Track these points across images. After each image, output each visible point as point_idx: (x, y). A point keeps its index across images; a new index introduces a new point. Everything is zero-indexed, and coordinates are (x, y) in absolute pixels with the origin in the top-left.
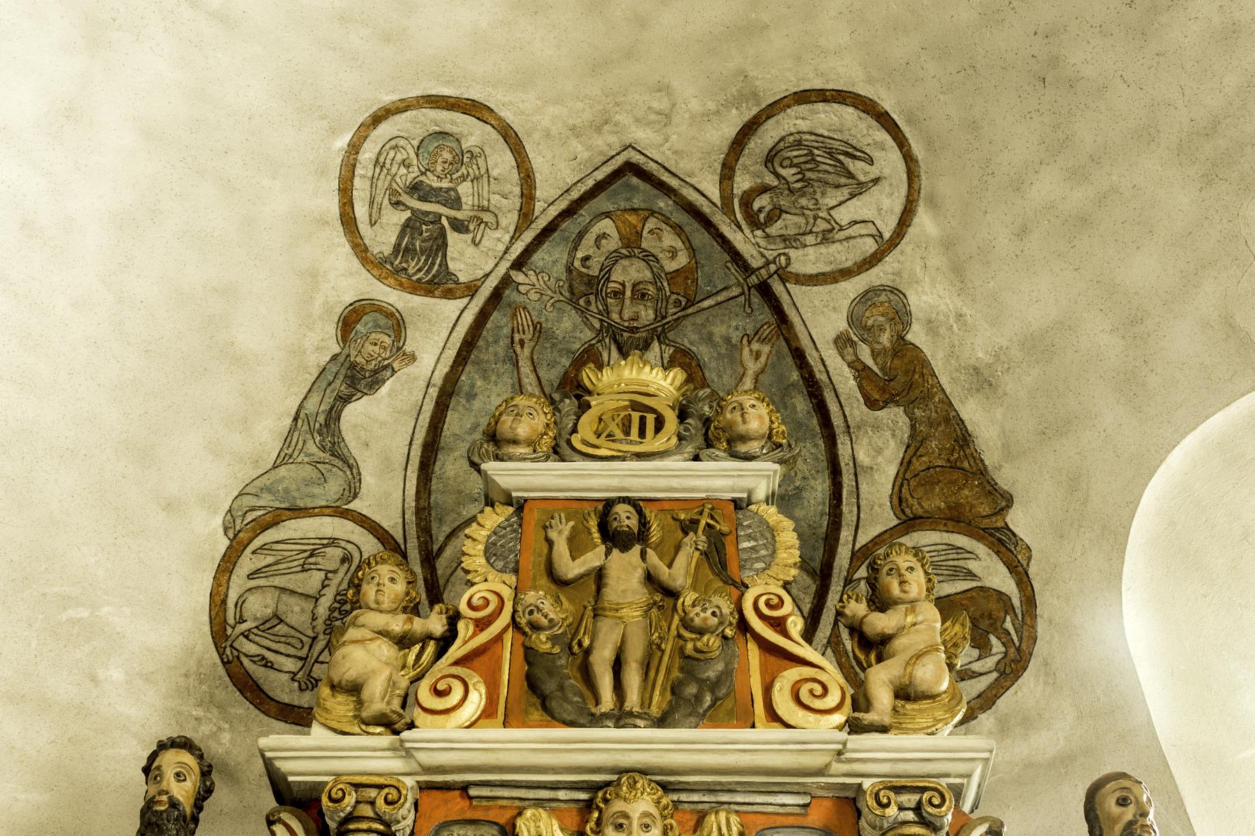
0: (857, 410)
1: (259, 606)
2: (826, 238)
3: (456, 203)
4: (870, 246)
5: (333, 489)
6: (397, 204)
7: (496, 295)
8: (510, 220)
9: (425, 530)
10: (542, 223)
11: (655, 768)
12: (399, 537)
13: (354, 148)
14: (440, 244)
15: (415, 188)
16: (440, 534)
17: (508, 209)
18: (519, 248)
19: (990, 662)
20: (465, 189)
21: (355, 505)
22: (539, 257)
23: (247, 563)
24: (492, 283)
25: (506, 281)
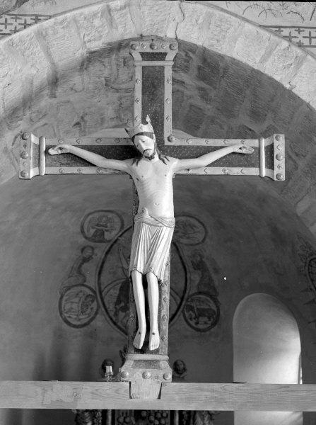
0: (192, 269)
1: (68, 307)
2: (188, 238)
3: (106, 227)
4: (197, 242)
5: (80, 281)
6: (93, 228)
7: (115, 242)
8: (118, 229)
9: (100, 288)
10: (125, 229)
11: (149, 293)
12: (94, 288)
13: (85, 220)
14: (103, 234)
15: (97, 225)
16: (103, 287)
17: (118, 226)
18: (120, 233)
19: (210, 322)
20: (108, 225)
21: (85, 283)
22: (125, 235)
23: (65, 298)
24: (114, 240)
25: (117, 239)
